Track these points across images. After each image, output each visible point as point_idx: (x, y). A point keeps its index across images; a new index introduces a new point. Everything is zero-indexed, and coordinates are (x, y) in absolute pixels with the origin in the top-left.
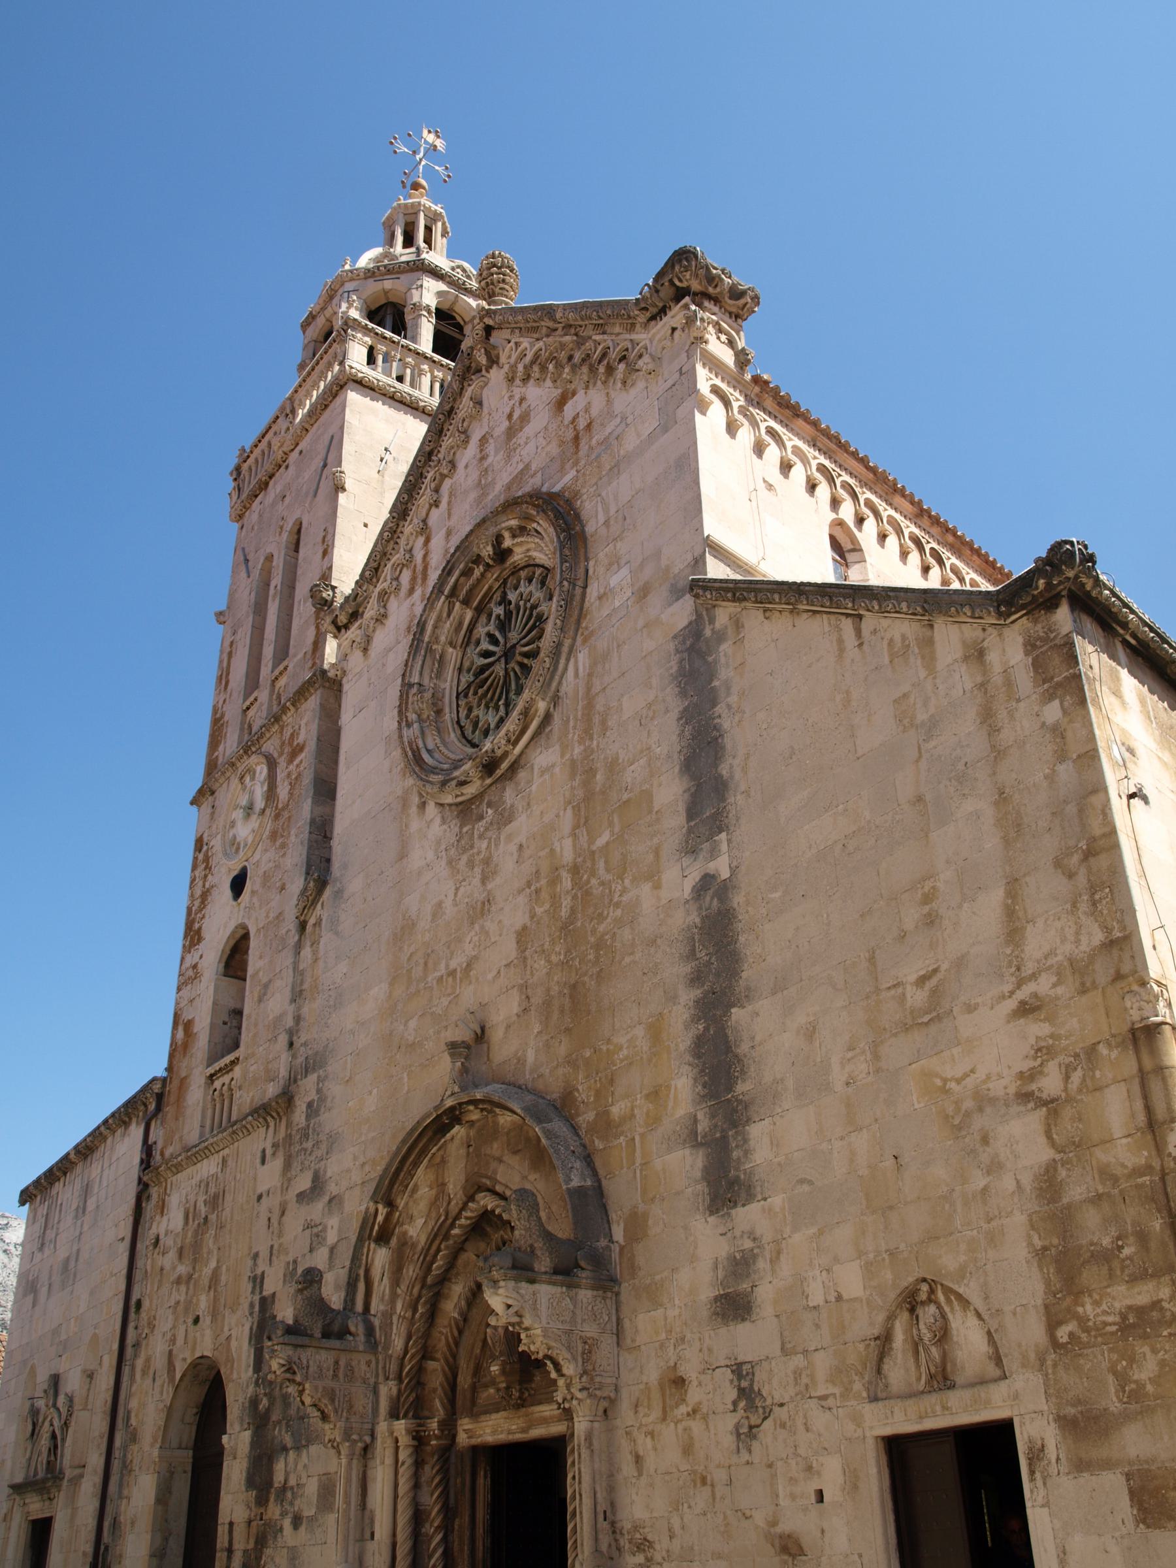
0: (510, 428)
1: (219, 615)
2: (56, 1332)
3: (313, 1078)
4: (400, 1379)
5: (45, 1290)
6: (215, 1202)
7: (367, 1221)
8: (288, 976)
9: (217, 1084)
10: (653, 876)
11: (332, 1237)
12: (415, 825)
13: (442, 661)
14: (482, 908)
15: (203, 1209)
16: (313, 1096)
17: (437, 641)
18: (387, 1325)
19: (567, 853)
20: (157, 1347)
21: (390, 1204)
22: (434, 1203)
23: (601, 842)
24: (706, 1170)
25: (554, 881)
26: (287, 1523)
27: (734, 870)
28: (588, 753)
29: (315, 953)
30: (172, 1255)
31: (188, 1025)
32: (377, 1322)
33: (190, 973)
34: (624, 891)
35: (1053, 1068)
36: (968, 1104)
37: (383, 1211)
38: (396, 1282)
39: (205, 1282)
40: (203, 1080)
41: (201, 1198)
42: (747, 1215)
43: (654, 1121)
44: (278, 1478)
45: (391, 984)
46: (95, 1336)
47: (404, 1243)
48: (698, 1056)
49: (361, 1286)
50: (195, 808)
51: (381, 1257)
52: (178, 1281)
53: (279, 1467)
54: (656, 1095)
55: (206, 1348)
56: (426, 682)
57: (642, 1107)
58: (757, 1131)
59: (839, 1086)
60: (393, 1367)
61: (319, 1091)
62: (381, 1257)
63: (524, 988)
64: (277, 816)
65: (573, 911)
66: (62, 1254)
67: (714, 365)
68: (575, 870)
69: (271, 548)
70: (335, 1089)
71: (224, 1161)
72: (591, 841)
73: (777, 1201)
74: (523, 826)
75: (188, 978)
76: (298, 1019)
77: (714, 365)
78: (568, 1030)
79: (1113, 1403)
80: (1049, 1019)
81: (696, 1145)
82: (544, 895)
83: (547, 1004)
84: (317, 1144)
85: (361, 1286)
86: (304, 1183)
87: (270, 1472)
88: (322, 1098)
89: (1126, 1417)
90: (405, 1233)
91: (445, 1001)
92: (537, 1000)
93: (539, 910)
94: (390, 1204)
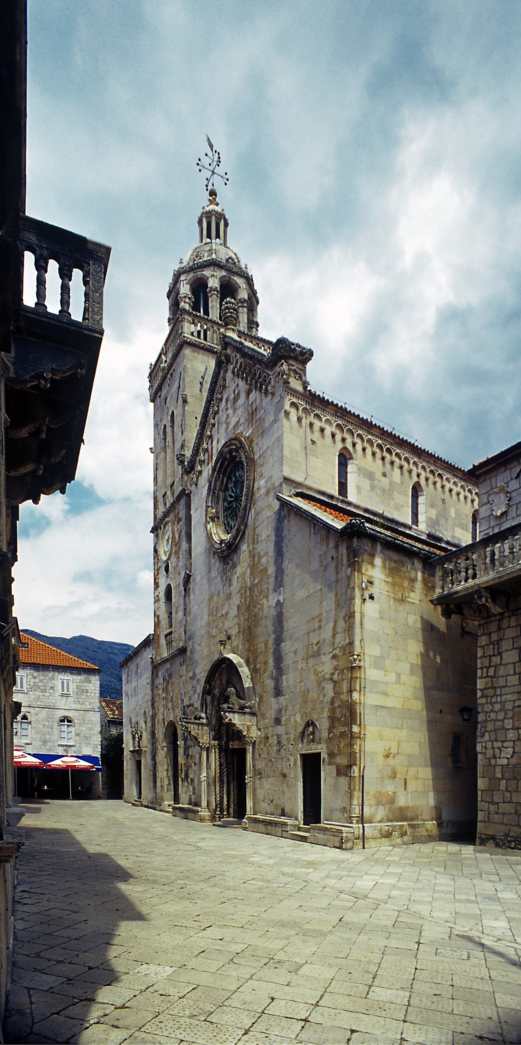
0: (234, 398)
1: (151, 449)
2: (135, 709)
3: (191, 642)
4: (214, 731)
5: (130, 696)
6: (170, 676)
7: (204, 688)
8: (182, 605)
9: (168, 638)
10: (267, 597)
11: (198, 692)
12: (212, 561)
13: (218, 497)
14: (229, 597)
15: (167, 678)
16: (191, 648)
17: (216, 489)
18: (211, 717)
19: (249, 585)
20: (160, 717)
21: (210, 685)
22: (220, 685)
23: (256, 581)
24: (274, 686)
25: (246, 592)
26: (193, 764)
27: (284, 600)
28: (254, 549)
29: (189, 600)
30: (161, 690)
31: (158, 617)
32: (209, 716)
33: (157, 598)
34: (261, 600)
35: (336, 673)
36: (321, 679)
37: (208, 687)
38: (213, 706)
39: (170, 699)
40: (164, 637)
41: (167, 675)
42: (281, 699)
43: (265, 671)
44: (190, 754)
45: (209, 615)
46: (145, 712)
47: (214, 695)
48: (274, 654)
49: (204, 706)
50: (152, 534)
51: (209, 698)
52: (163, 698)
53: (190, 751)
54: (266, 663)
55: (171, 718)
56: (213, 505)
57: (263, 667)
58: (284, 677)
59: (300, 669)
60: (213, 728)
61: (193, 646)
62: (209, 698)
63: (238, 624)
64: (176, 545)
65: (249, 602)
66: (133, 685)
67: (294, 392)
68: (250, 589)
69: (165, 422)
70: (197, 647)
71: (171, 664)
72: (254, 581)
73: (286, 697)
74: (239, 570)
75: (157, 600)
76: (186, 621)
77: (294, 392)
78: (248, 640)
79: (336, 751)
80: (337, 661)
81: (273, 679)
82: (243, 595)
83: (244, 631)
84: (193, 662)
85: (204, 706)
86: (191, 674)
87: (189, 752)
88: (194, 648)
89: (338, 754)
90: (214, 693)
91: (221, 624)
92: (242, 629)
93: (242, 600)
94: (210, 685)
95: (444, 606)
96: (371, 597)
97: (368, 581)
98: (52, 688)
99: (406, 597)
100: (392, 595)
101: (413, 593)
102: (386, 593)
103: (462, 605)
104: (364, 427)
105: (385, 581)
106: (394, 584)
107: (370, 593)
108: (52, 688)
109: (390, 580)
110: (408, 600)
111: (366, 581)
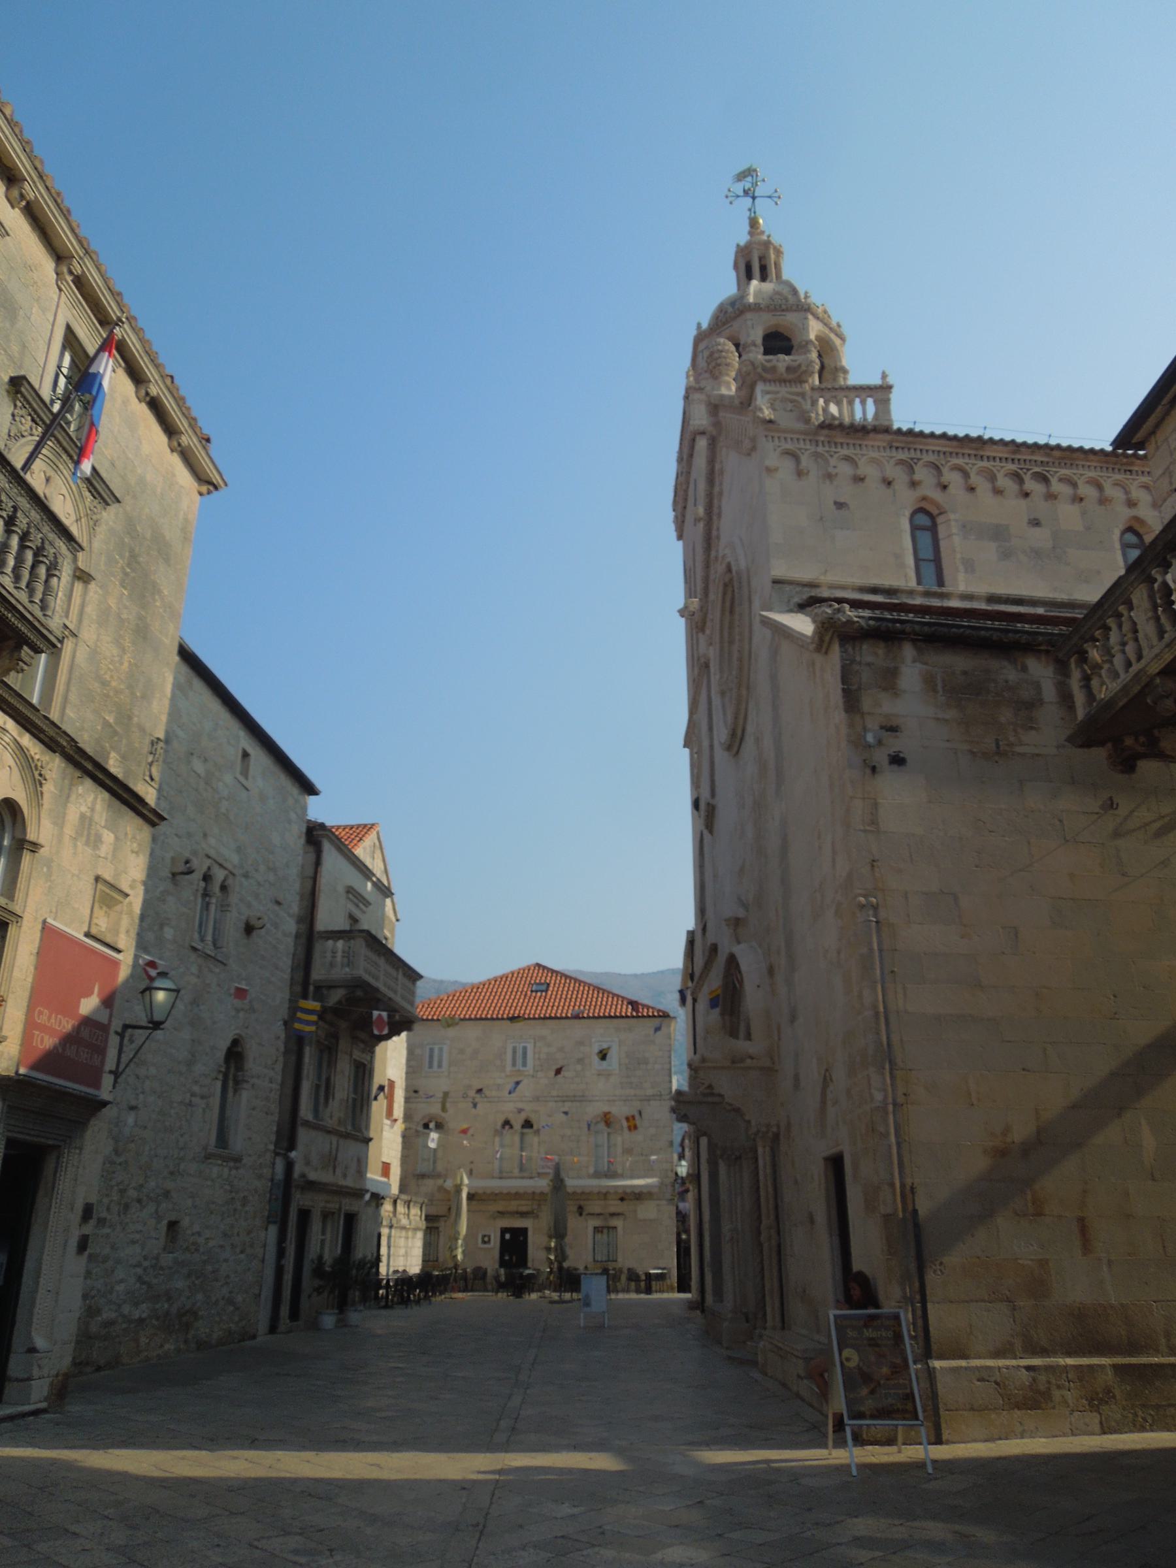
95: (1109, 745)
96: (897, 760)
97: (882, 727)
99: (1011, 745)
101: (1033, 732)
103: (1156, 732)
104: (967, 451)
105: (938, 719)
107: (891, 751)
109: (951, 714)
110: (1018, 749)
111: (877, 727)
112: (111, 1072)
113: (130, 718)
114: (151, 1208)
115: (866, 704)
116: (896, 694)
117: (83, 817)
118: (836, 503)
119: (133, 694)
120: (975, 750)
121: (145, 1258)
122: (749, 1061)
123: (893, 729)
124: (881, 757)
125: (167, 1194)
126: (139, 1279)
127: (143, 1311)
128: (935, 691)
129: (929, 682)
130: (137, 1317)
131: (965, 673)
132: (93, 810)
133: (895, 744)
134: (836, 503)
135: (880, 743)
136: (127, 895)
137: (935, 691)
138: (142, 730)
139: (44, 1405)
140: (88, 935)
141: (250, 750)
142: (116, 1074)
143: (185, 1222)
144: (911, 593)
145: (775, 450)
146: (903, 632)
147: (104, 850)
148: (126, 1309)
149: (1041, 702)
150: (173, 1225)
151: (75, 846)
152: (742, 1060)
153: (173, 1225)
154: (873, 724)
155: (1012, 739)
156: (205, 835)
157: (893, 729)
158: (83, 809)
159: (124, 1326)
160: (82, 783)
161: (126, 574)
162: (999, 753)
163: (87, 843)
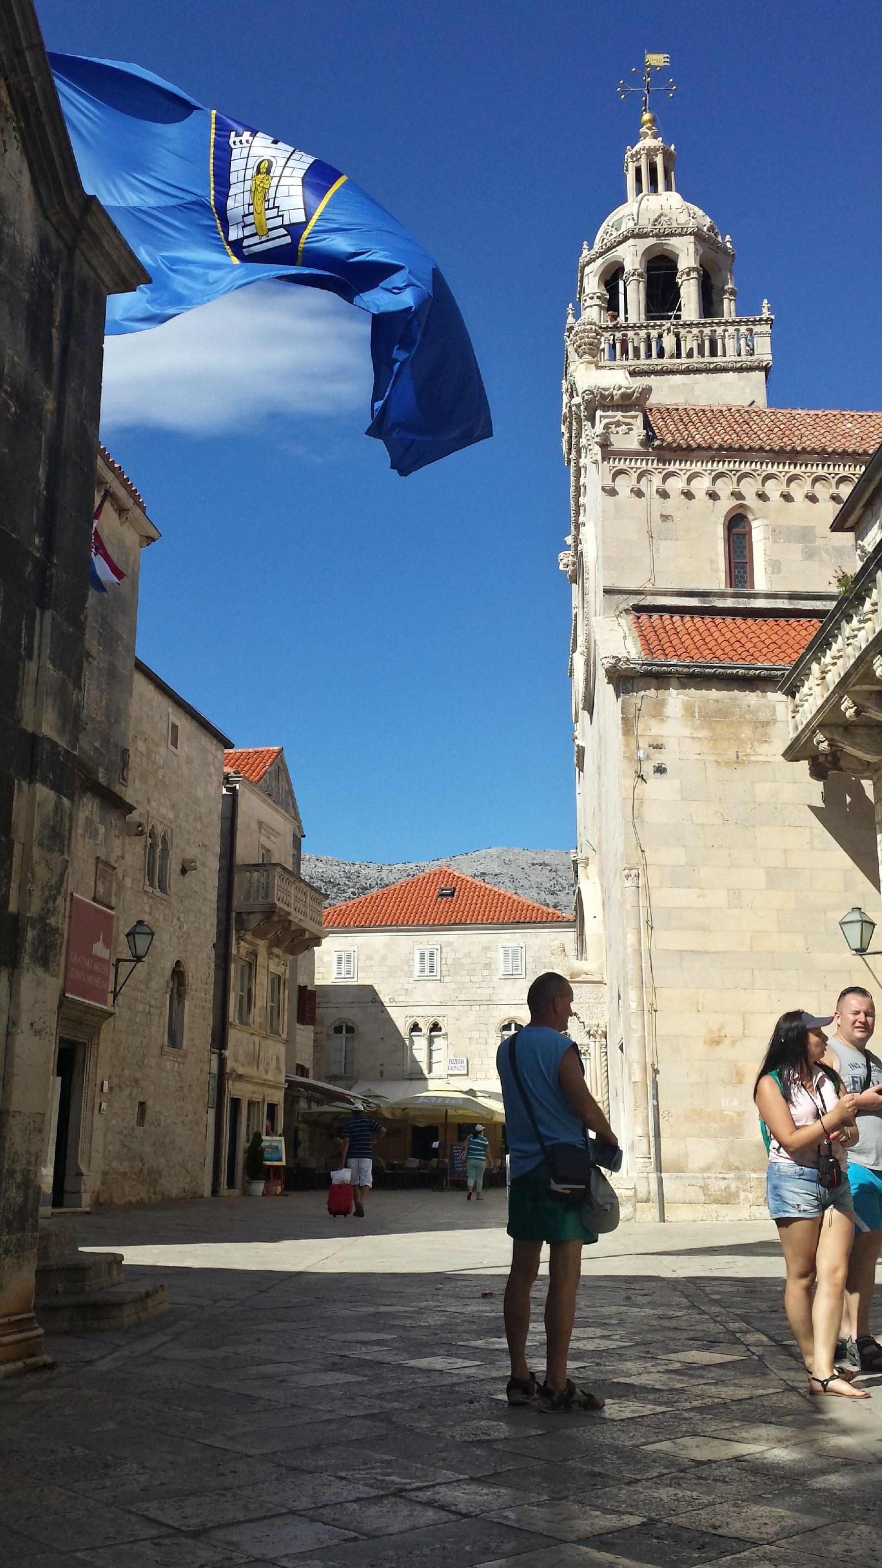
95: (810, 760)
96: (660, 770)
97: (650, 746)
98: (487, 966)
100: (712, 758)
101: (766, 745)
102: (698, 757)
105: (693, 738)
106: (714, 740)
108: (487, 966)
109: (704, 733)
111: (646, 746)
112: (111, 992)
113: (109, 740)
114: (127, 1091)
115: (641, 727)
116: (662, 719)
117: (87, 817)
118: (662, 516)
119: (109, 721)
120: (720, 760)
121: (125, 1128)
122: (584, 976)
123: (658, 747)
124: (648, 769)
125: (137, 1081)
126: (122, 1143)
127: (125, 1167)
128: (692, 715)
129: (689, 711)
130: (122, 1170)
131: (717, 701)
132: (92, 812)
133: (659, 758)
134: (662, 516)
135: (648, 757)
136: (115, 868)
137: (692, 715)
138: (116, 746)
139: (88, 1209)
140: (94, 899)
141: (178, 723)
142: (116, 994)
143: (150, 1103)
144: (722, 595)
145: (610, 470)
146: (670, 673)
147: (101, 837)
148: (115, 1164)
149: (775, 721)
150: (142, 1104)
151: (84, 840)
152: (579, 975)
153: (142, 1104)
154: (644, 744)
155: (749, 751)
156: (149, 800)
157: (658, 747)
158: (87, 813)
159: (115, 1176)
160: (85, 795)
161: (100, 634)
162: (738, 760)
163: (90, 838)
